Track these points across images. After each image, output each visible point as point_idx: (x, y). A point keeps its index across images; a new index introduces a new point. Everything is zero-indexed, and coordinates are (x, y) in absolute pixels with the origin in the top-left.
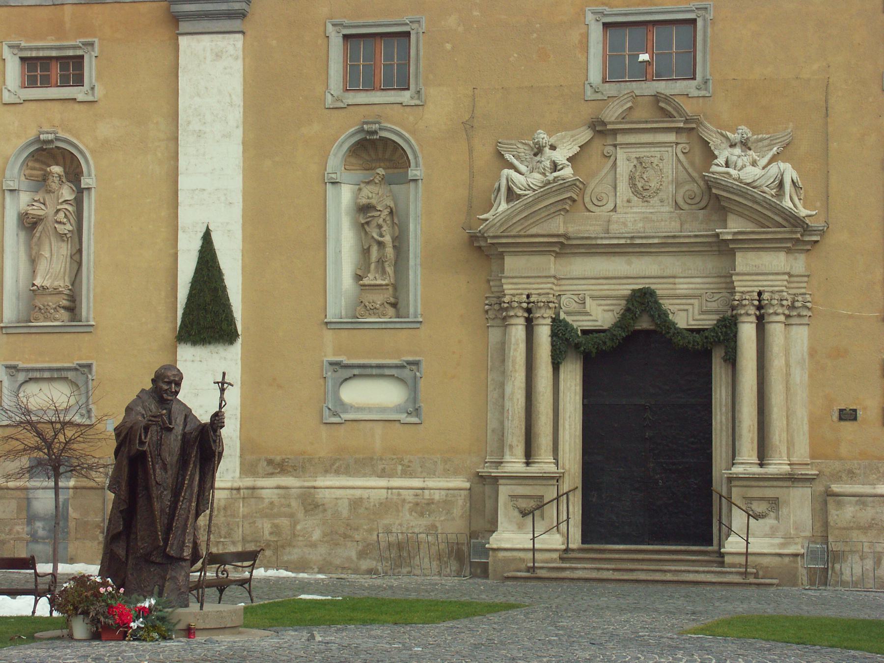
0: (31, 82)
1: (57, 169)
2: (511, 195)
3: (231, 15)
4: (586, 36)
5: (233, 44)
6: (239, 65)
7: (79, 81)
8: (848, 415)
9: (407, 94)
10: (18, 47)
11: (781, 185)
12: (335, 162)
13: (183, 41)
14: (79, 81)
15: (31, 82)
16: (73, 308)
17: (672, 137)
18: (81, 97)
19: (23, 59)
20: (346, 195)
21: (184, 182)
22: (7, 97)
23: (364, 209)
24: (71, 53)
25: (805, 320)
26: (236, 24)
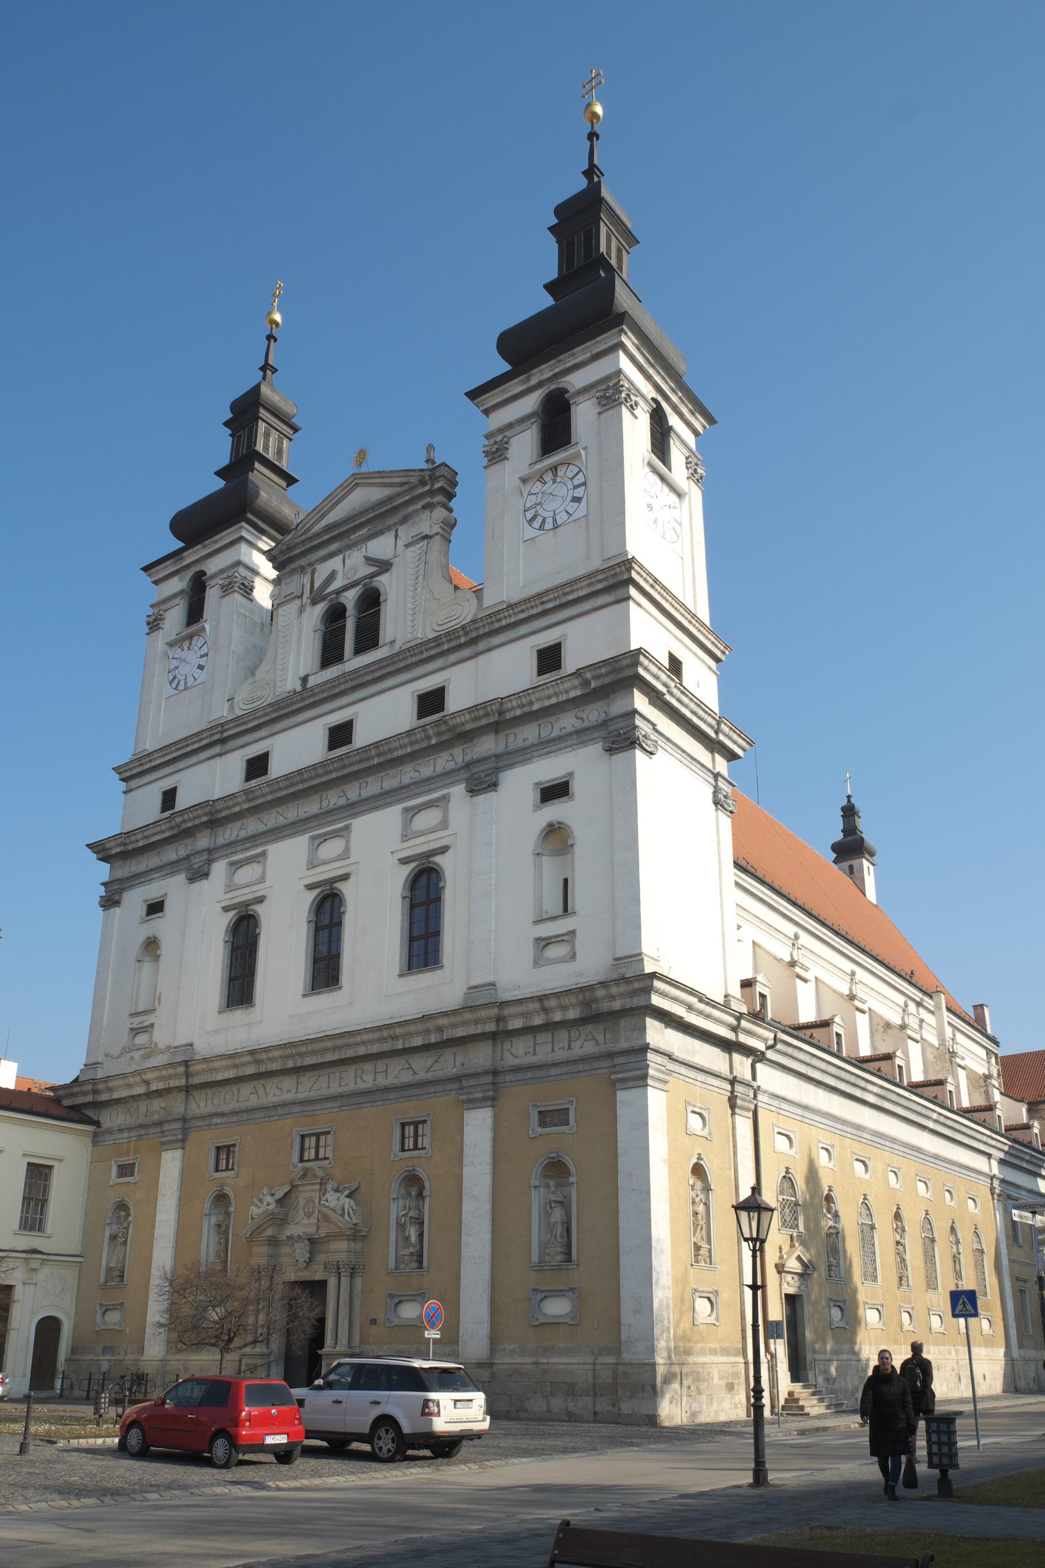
0: (120, 1175)
1: (123, 1213)
2: (253, 1218)
3: (177, 1141)
4: (292, 1141)
5: (178, 1154)
6: (178, 1163)
7: (132, 1174)
8: (374, 1321)
9: (233, 1172)
10: (117, 1162)
11: (344, 1209)
12: (207, 1205)
13: (163, 1153)
14: (132, 1174)
15: (120, 1175)
16: (122, 1277)
17: (318, 1187)
18: (132, 1181)
19: (119, 1166)
20: (214, 1220)
21: (158, 1217)
22: (111, 1183)
23: (219, 1226)
24: (131, 1162)
25: (360, 1274)
26: (179, 1145)
